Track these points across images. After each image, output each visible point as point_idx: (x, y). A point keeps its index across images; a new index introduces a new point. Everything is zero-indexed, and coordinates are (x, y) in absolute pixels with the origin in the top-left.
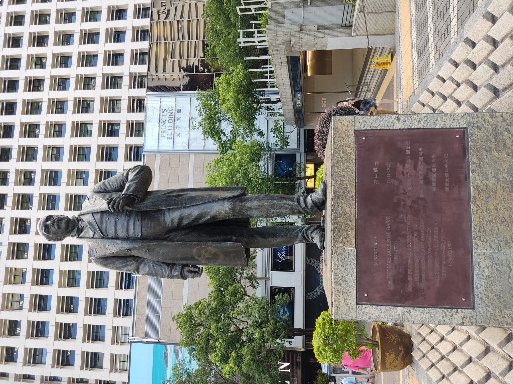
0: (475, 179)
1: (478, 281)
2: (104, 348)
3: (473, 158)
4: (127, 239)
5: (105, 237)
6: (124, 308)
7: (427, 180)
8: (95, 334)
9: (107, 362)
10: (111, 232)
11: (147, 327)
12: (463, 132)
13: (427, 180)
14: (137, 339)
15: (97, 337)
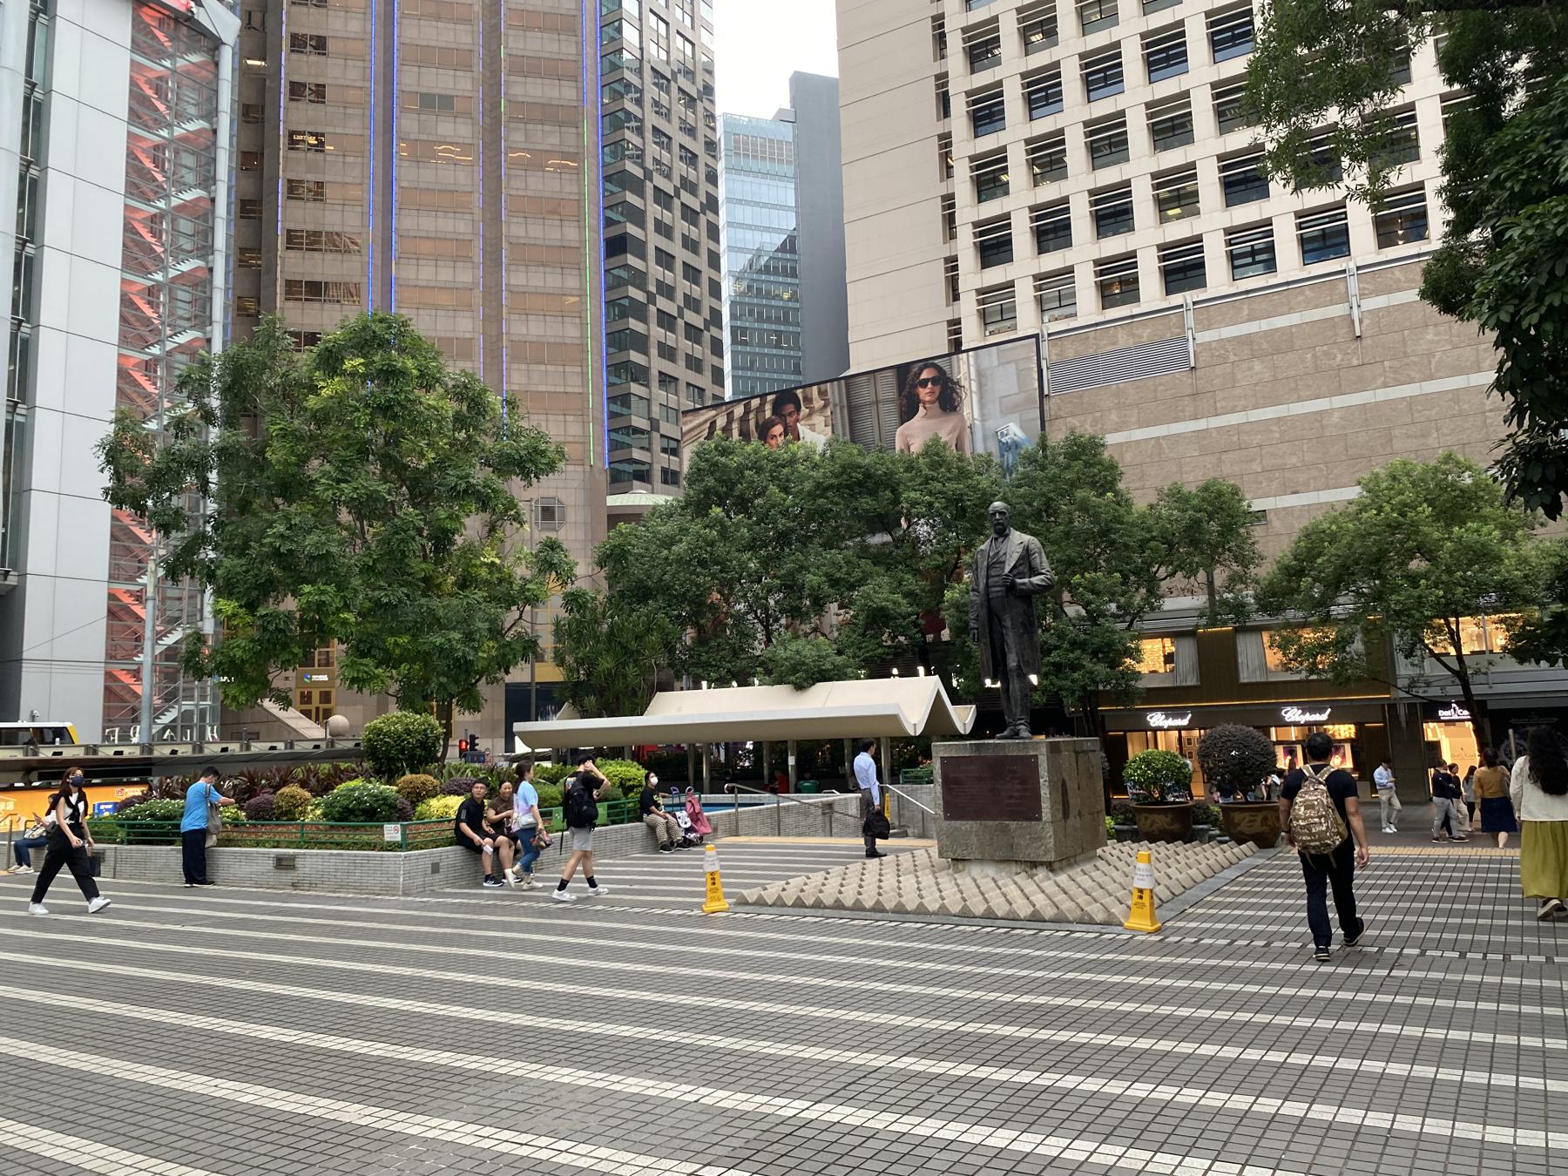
0: (1013, 825)
1: (958, 823)
2: (1025, 261)
3: (1025, 824)
4: (987, 586)
5: (988, 567)
6: (1117, 281)
7: (1011, 797)
8: (1052, 229)
9: (996, 275)
10: (992, 573)
11: (1070, 361)
12: (1040, 819)
13: (1011, 797)
14: (1044, 346)
15: (1046, 232)
